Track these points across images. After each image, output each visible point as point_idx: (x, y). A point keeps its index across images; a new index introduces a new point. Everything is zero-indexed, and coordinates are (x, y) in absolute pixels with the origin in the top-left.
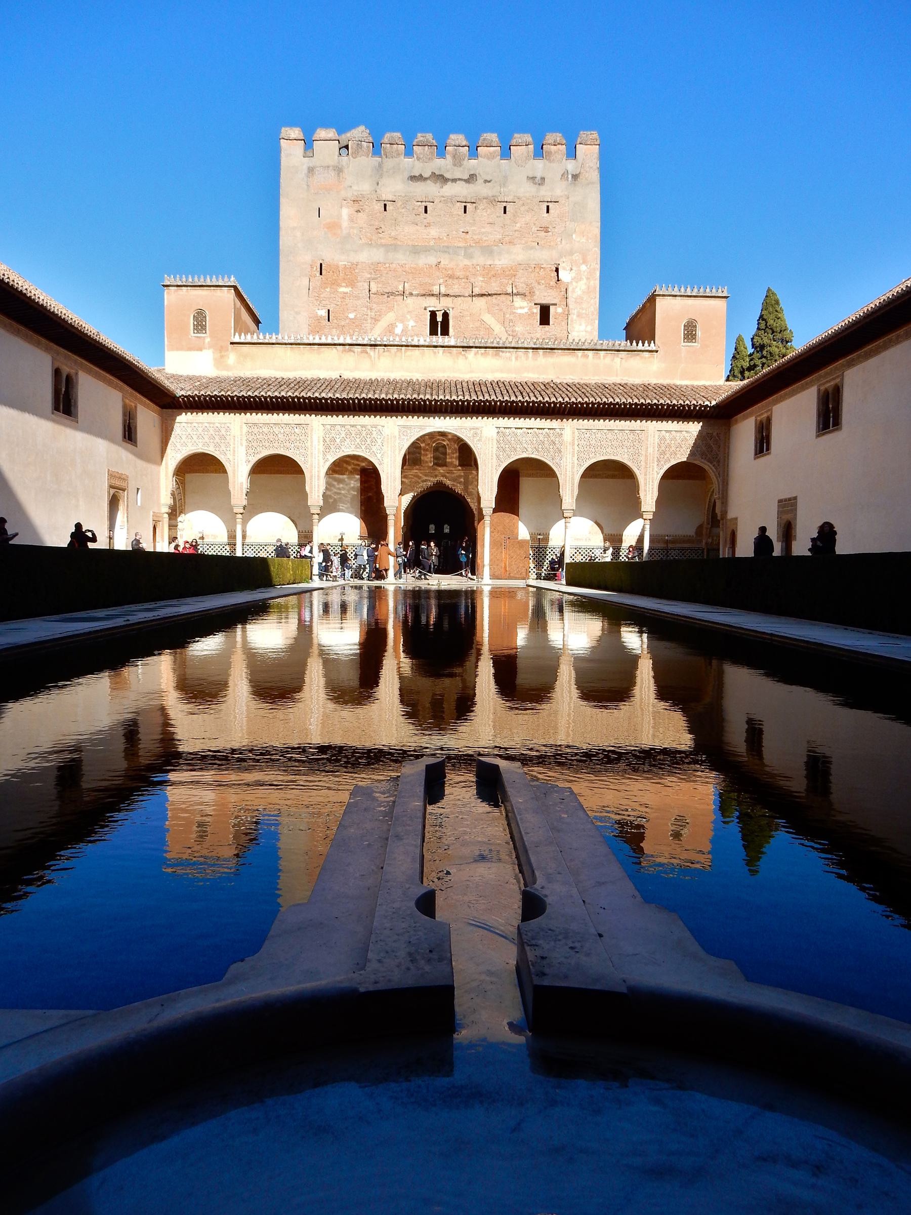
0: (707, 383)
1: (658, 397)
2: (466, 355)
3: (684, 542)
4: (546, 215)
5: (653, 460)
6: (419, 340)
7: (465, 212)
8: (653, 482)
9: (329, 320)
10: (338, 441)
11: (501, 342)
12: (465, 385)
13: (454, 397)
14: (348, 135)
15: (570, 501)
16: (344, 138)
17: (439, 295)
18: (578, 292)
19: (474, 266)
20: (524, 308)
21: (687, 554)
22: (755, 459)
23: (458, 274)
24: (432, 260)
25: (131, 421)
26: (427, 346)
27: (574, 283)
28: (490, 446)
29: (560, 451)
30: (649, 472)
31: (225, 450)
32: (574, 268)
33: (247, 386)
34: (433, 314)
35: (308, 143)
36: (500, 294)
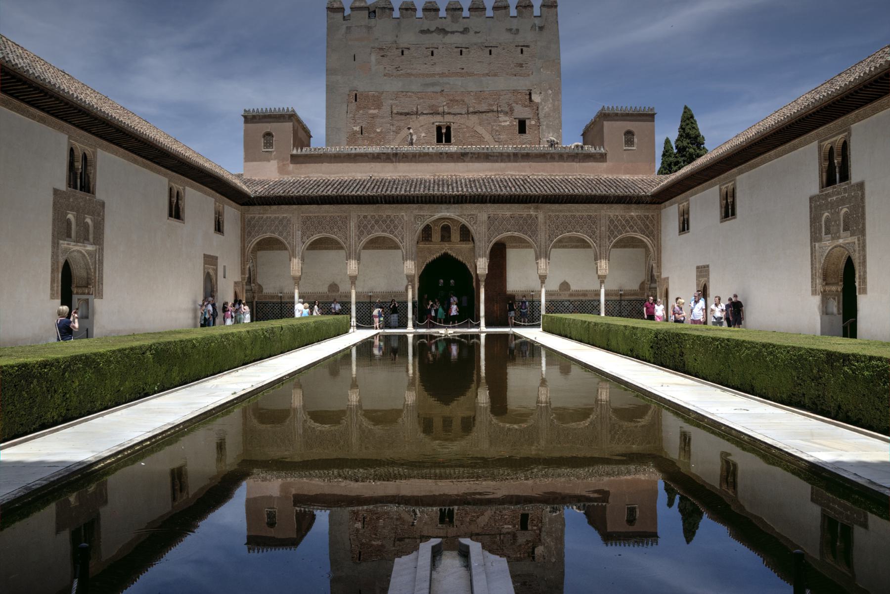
3: (633, 295)
4: (521, 55)
6: (429, 148)
7: (461, 54)
9: (362, 134)
10: (369, 227)
12: (463, 181)
17: (443, 114)
18: (546, 109)
19: (469, 92)
20: (506, 121)
23: (456, 98)
24: (438, 89)
25: (220, 217)
32: (543, 93)
33: (303, 187)
34: (439, 128)
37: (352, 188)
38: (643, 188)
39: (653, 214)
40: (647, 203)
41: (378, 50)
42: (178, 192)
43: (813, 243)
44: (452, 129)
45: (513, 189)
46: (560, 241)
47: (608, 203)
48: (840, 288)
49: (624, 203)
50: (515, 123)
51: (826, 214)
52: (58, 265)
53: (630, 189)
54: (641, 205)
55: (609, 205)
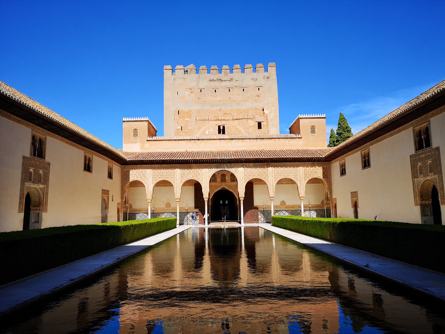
0: (321, 148)
1: (302, 155)
2: (232, 142)
5: (302, 177)
7: (229, 91)
8: (303, 186)
10: (186, 175)
11: (244, 137)
12: (232, 152)
13: (228, 158)
14: (188, 67)
15: (273, 193)
16: (186, 68)
20: (252, 123)
21: (319, 212)
22: (341, 177)
23: (228, 112)
24: (218, 108)
25: (111, 171)
26: (218, 139)
27: (270, 114)
28: (242, 175)
29: (268, 176)
30: (302, 182)
31: (144, 179)
34: (219, 127)
35: (173, 70)
36: (243, 119)
37: (177, 156)
38: (321, 154)
39: (326, 166)
40: (323, 161)
41: (189, 89)
42: (89, 158)
43: (414, 179)
44: (225, 128)
45: (256, 156)
46: (280, 181)
47: (304, 161)
48: (430, 202)
49: (311, 161)
50: (256, 124)
51: (420, 164)
52: (23, 195)
53: (314, 155)
54: (320, 162)
55: (304, 163)
